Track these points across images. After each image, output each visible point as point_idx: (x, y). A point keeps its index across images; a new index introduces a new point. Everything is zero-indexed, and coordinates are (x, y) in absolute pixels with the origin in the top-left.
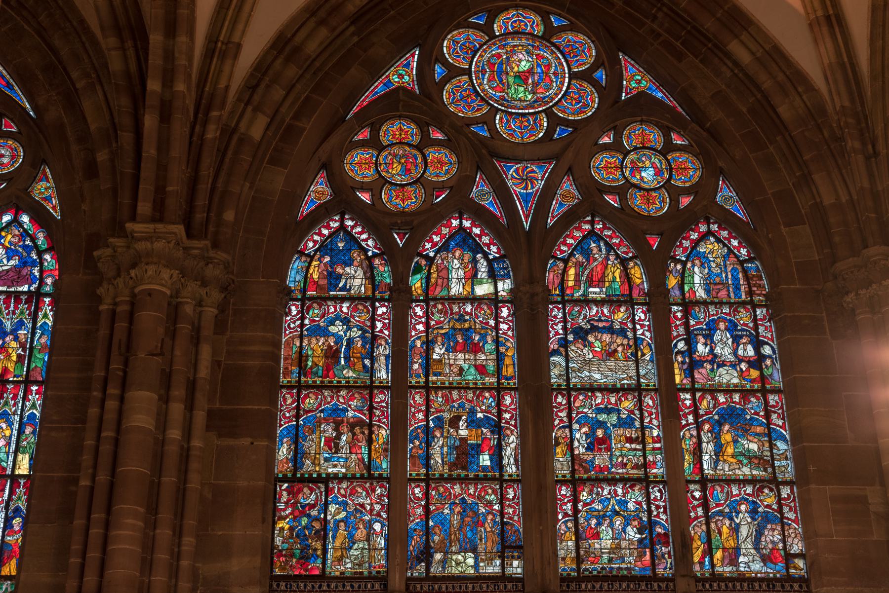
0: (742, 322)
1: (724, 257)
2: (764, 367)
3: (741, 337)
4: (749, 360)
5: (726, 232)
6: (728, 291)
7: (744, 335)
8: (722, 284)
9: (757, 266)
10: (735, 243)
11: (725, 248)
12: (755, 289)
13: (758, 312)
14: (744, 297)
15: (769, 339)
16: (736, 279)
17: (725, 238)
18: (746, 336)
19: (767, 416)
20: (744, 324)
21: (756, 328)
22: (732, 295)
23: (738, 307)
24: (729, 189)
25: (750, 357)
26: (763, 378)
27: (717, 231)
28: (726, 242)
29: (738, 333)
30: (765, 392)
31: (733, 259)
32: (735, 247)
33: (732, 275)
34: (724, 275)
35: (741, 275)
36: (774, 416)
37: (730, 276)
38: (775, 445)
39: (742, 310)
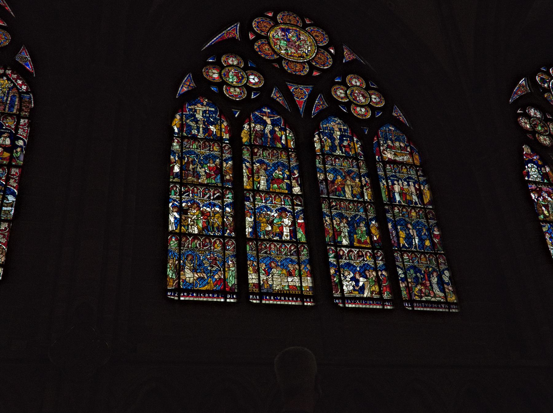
0: (7, 124)
1: (9, 88)
2: (15, 152)
3: (4, 133)
4: (5, 147)
5: (16, 76)
6: (5, 107)
7: (6, 132)
8: (3, 103)
9: (31, 97)
10: (20, 82)
11: (12, 84)
12: (24, 108)
13: (22, 121)
14: (15, 111)
15: (24, 137)
16: (13, 101)
17: (14, 79)
18: (8, 133)
19: (7, 180)
20: (8, 126)
21: (17, 129)
22: (7, 109)
23: (7, 116)
24: (26, 53)
25: (7, 145)
26: (11, 158)
27: (9, 74)
28: (14, 81)
29: (2, 130)
30: (10, 166)
31: (15, 91)
32: (18, 84)
33: (11, 99)
34: (5, 98)
35: (17, 99)
36: (12, 181)
37: (9, 99)
38: (7, 198)
39: (9, 118)
